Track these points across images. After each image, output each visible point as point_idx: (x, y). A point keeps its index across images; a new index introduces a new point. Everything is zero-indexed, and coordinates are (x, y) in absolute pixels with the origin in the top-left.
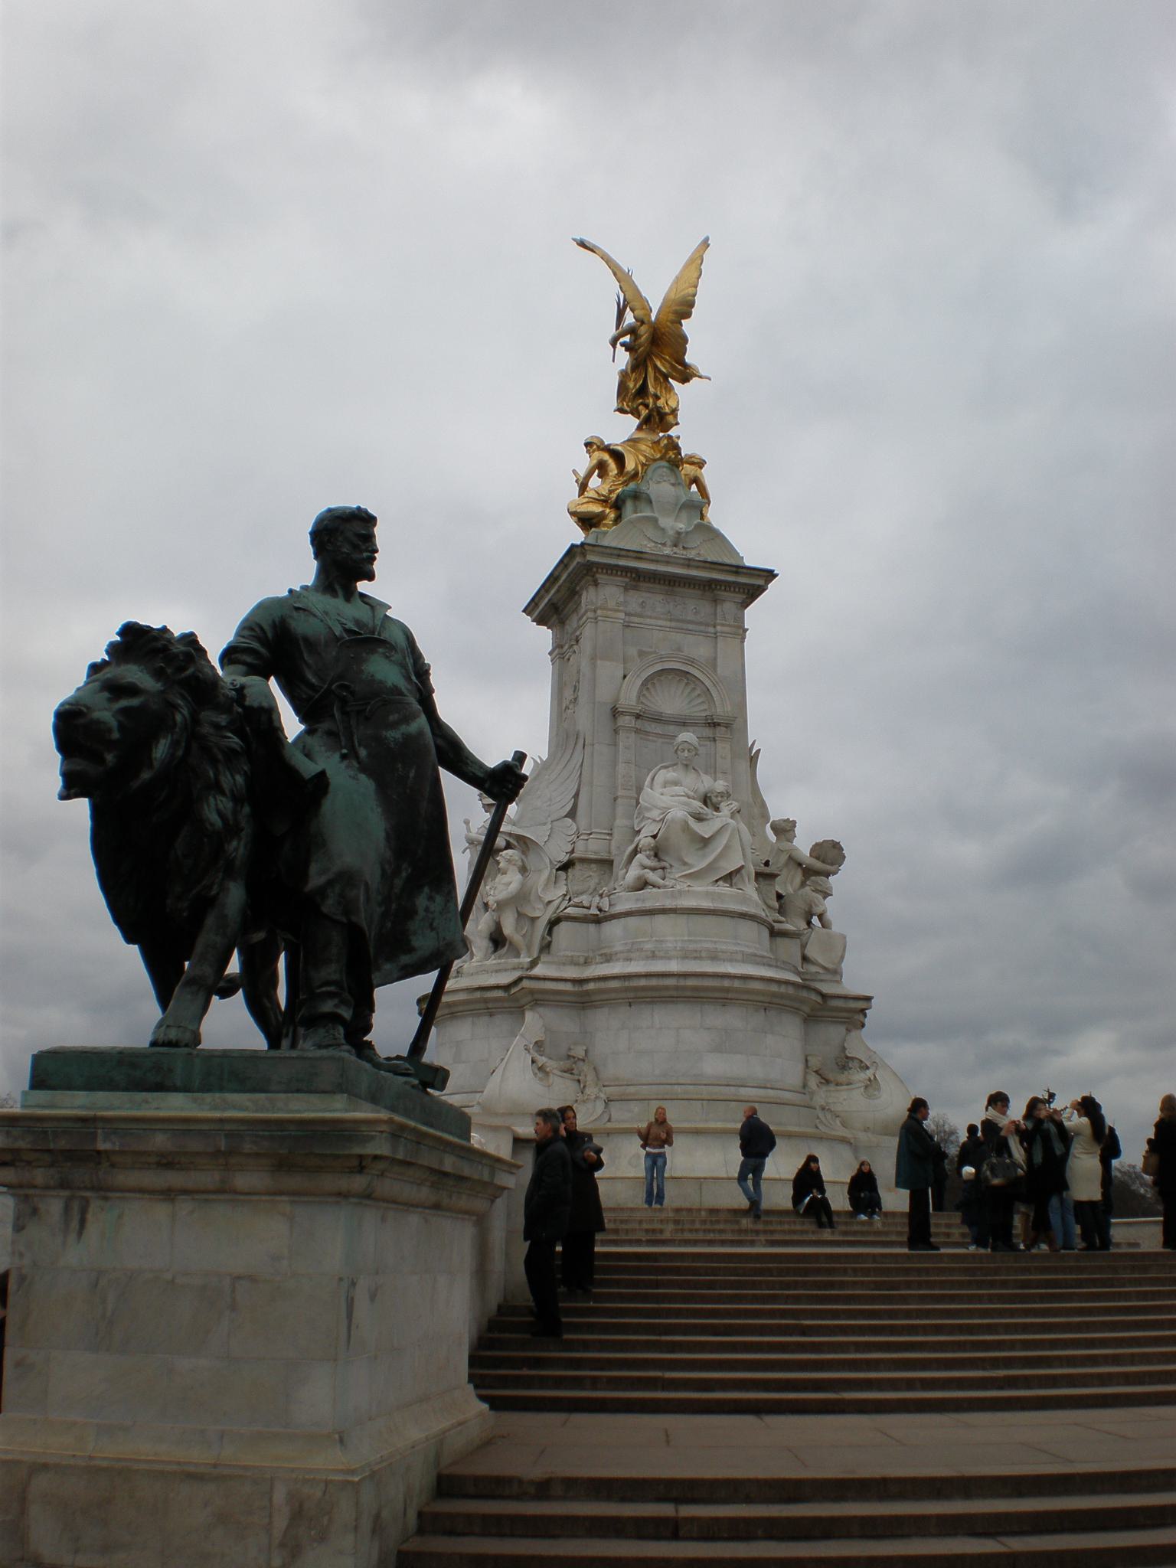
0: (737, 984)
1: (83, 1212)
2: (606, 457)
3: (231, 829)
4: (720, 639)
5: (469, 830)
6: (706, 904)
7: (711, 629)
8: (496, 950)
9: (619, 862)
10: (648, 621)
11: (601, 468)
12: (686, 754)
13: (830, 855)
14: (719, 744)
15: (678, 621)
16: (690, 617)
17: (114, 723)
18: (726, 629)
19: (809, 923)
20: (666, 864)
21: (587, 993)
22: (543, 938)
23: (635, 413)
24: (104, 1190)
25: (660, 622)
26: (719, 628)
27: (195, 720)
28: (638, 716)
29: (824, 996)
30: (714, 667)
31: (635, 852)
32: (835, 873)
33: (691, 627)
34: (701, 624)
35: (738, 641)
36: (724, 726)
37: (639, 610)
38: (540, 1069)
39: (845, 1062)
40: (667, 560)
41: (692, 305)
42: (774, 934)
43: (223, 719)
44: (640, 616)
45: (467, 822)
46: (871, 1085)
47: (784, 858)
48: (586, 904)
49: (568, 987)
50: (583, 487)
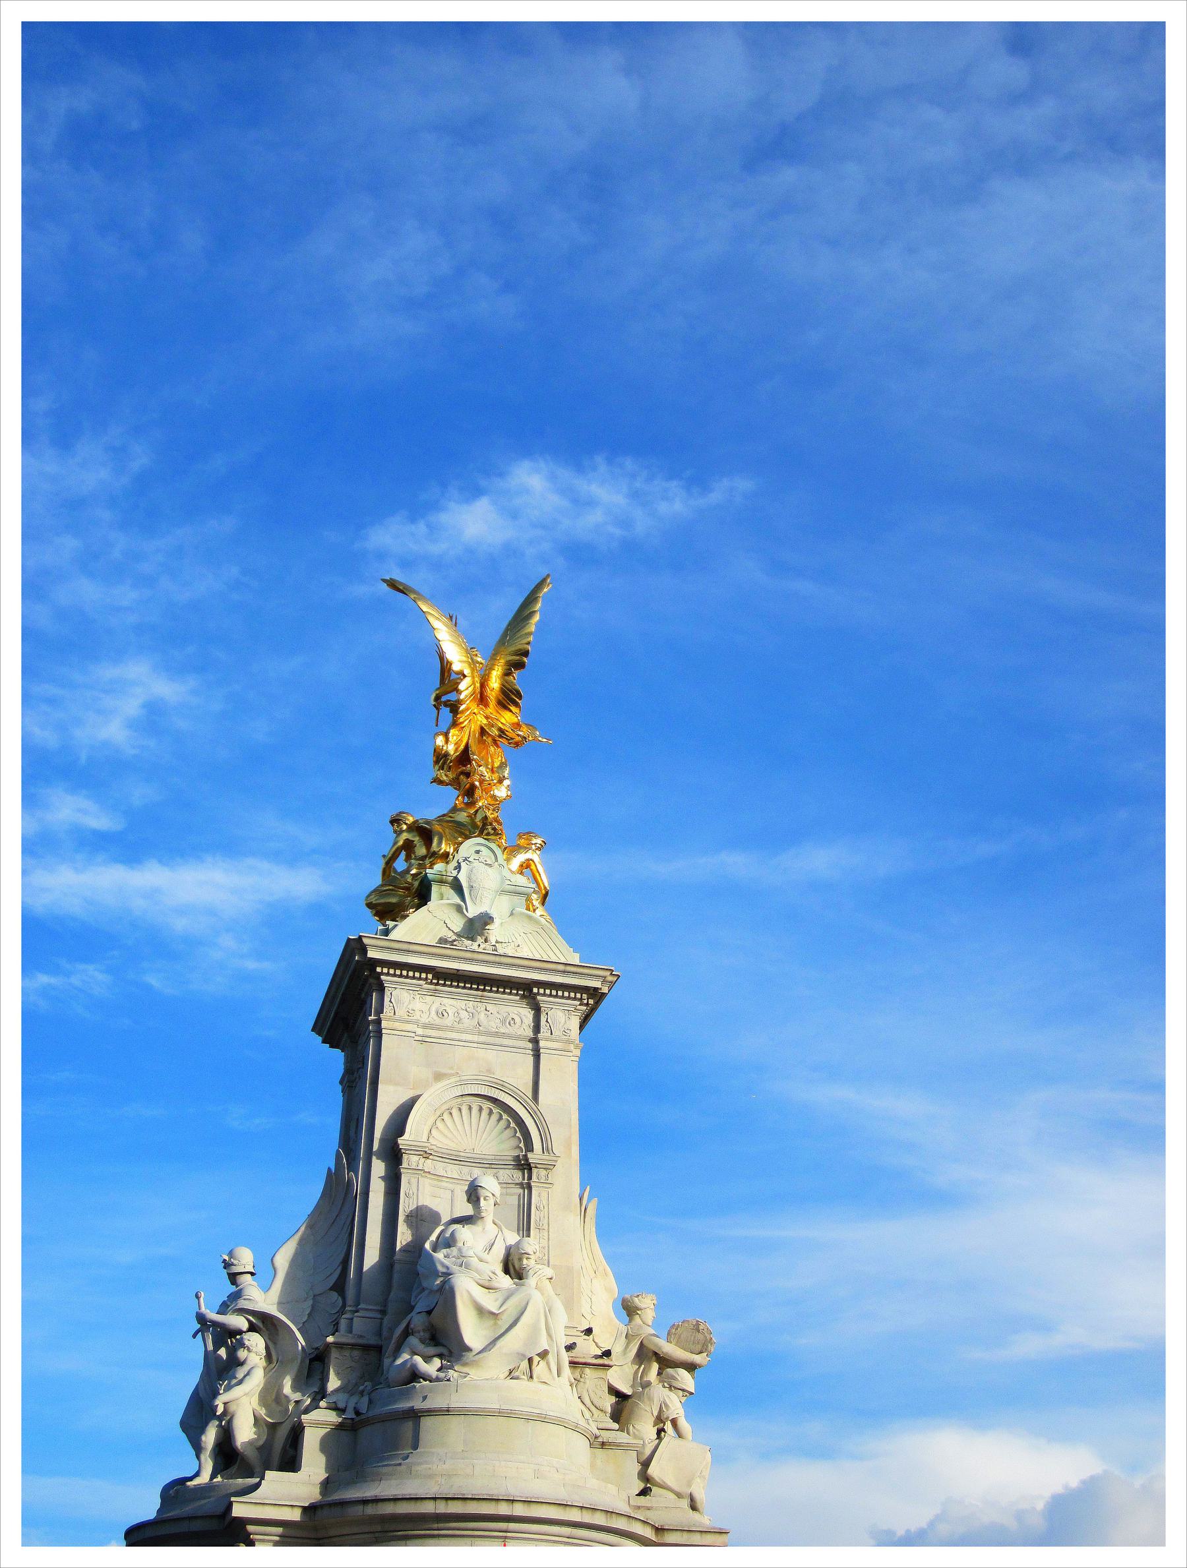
11: (408, 846)
15: (488, 1034)
22: (284, 1449)
23: (455, 783)
48: (341, 1405)
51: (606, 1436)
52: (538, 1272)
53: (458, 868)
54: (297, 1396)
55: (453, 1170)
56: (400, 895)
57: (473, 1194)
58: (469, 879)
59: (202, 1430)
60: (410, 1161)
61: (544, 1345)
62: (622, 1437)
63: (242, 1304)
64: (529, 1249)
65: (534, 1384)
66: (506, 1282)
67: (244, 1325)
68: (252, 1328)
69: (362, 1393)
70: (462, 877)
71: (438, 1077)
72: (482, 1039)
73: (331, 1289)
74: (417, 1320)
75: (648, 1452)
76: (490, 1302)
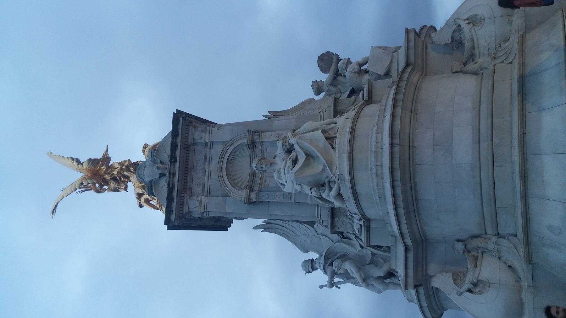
4: (213, 140)
5: (325, 286)
6: (345, 157)
7: (209, 145)
10: (206, 182)
12: (263, 166)
13: (327, 61)
14: (264, 140)
16: (203, 157)
19: (366, 72)
20: (327, 180)
21: (414, 241)
25: (207, 173)
26: (207, 141)
28: (251, 190)
29: (407, 65)
30: (225, 143)
31: (321, 198)
32: (338, 56)
33: (208, 157)
34: (206, 151)
35: (214, 130)
36: (253, 136)
37: (201, 187)
38: (475, 285)
39: (456, 43)
42: (370, 101)
44: (204, 187)
45: (321, 287)
46: (474, 21)
47: (332, 89)
48: (359, 227)
49: (411, 255)
68: (331, 264)
72: (207, 167)
73: (313, 227)
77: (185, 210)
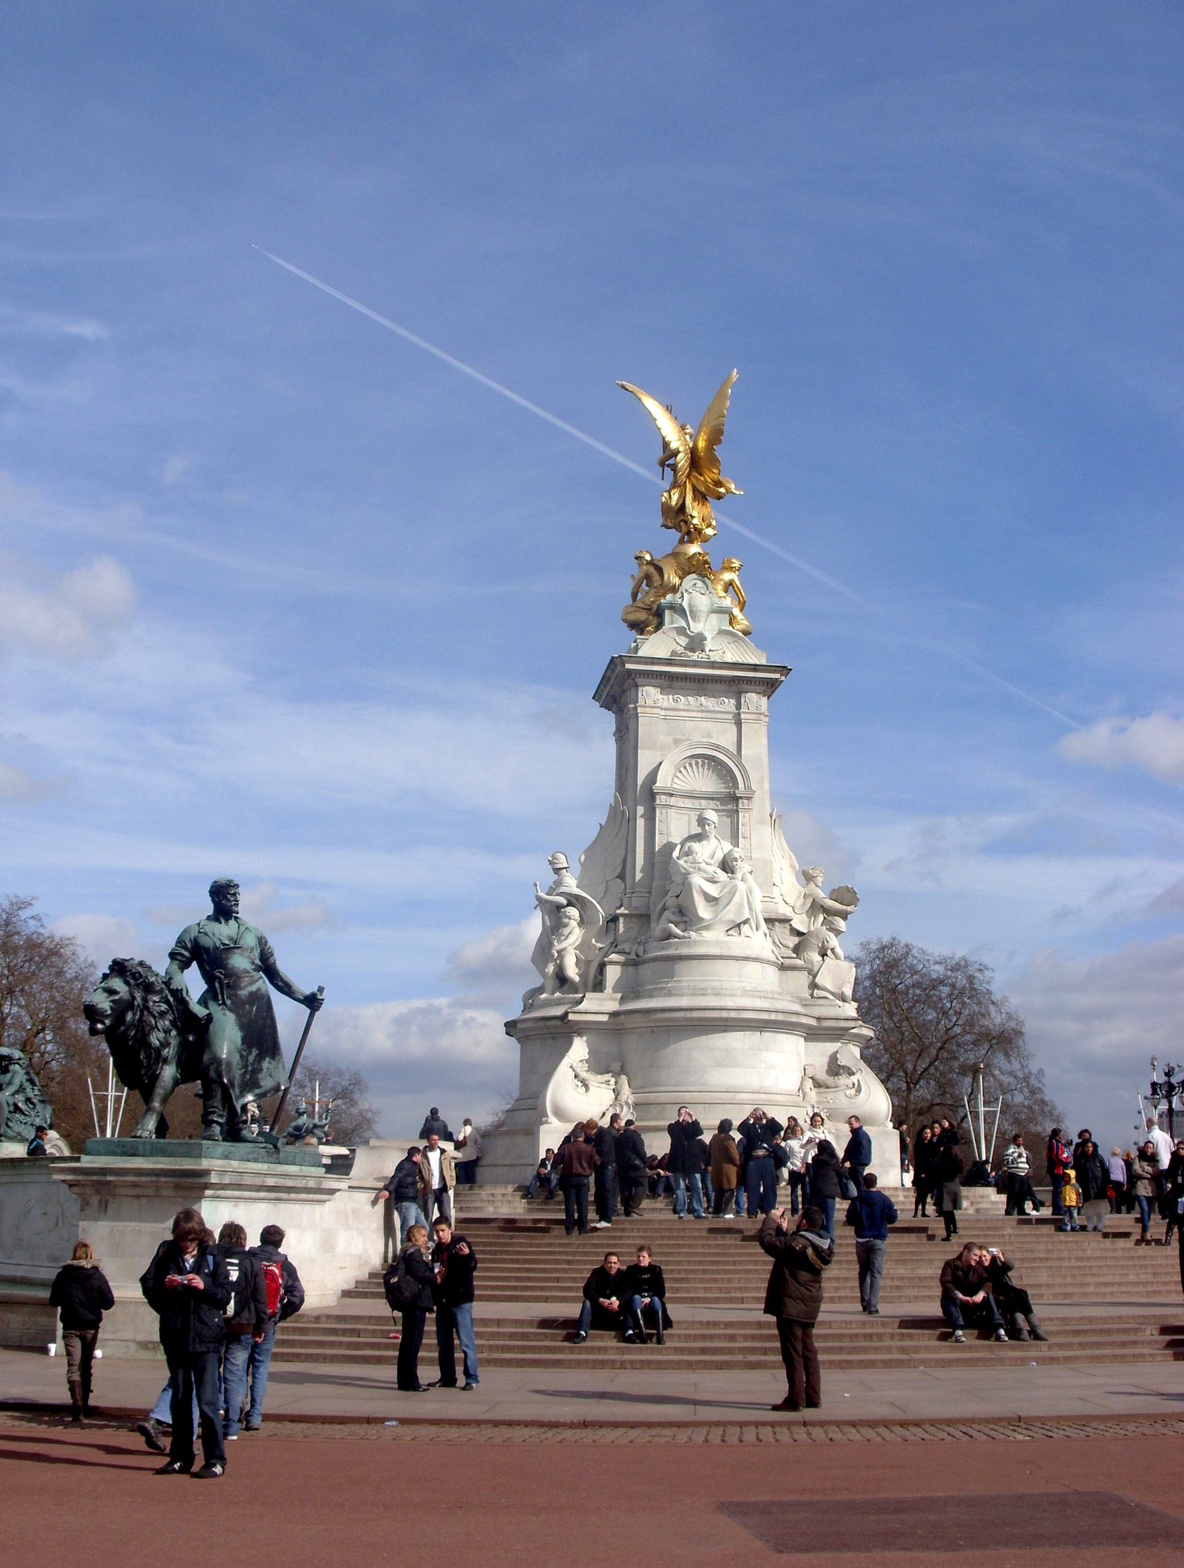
0: (733, 1015)
1: (106, 1204)
2: (652, 570)
3: (165, 1044)
8: (562, 986)
9: (654, 917)
11: (648, 577)
17: (108, 1008)
18: (748, 716)
23: (678, 528)
24: (114, 1196)
27: (145, 1000)
33: (719, 716)
40: (695, 664)
41: (722, 433)
43: (156, 998)
50: (634, 596)
51: (787, 961)
52: (743, 868)
53: (682, 597)
54: (599, 945)
55: (688, 803)
56: (648, 619)
57: (702, 821)
58: (690, 606)
59: (545, 966)
60: (661, 800)
61: (747, 915)
62: (799, 962)
63: (563, 889)
64: (737, 855)
65: (742, 938)
66: (722, 876)
67: (565, 902)
68: (570, 904)
69: (639, 943)
70: (685, 604)
71: (677, 742)
74: (670, 901)
75: (816, 969)
76: (713, 890)
77: (639, 680)
